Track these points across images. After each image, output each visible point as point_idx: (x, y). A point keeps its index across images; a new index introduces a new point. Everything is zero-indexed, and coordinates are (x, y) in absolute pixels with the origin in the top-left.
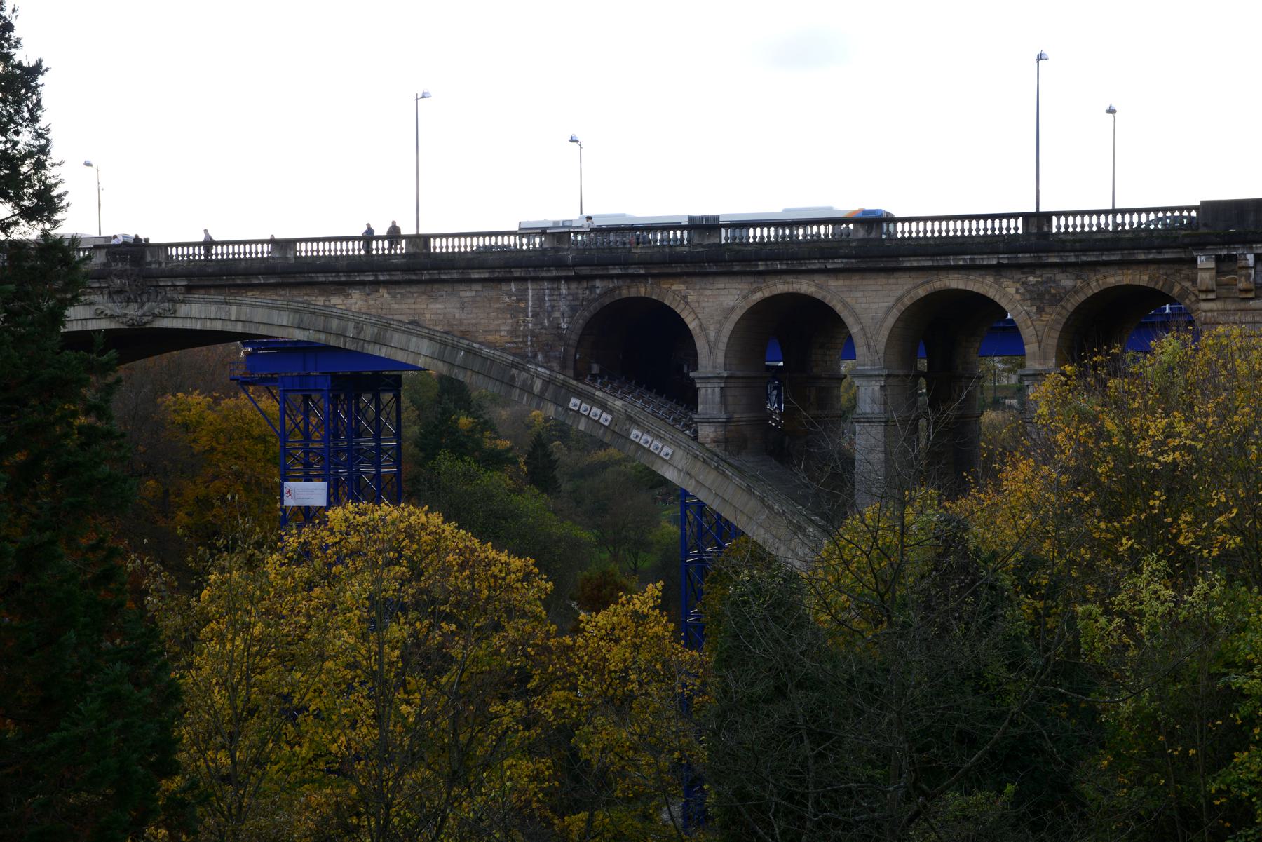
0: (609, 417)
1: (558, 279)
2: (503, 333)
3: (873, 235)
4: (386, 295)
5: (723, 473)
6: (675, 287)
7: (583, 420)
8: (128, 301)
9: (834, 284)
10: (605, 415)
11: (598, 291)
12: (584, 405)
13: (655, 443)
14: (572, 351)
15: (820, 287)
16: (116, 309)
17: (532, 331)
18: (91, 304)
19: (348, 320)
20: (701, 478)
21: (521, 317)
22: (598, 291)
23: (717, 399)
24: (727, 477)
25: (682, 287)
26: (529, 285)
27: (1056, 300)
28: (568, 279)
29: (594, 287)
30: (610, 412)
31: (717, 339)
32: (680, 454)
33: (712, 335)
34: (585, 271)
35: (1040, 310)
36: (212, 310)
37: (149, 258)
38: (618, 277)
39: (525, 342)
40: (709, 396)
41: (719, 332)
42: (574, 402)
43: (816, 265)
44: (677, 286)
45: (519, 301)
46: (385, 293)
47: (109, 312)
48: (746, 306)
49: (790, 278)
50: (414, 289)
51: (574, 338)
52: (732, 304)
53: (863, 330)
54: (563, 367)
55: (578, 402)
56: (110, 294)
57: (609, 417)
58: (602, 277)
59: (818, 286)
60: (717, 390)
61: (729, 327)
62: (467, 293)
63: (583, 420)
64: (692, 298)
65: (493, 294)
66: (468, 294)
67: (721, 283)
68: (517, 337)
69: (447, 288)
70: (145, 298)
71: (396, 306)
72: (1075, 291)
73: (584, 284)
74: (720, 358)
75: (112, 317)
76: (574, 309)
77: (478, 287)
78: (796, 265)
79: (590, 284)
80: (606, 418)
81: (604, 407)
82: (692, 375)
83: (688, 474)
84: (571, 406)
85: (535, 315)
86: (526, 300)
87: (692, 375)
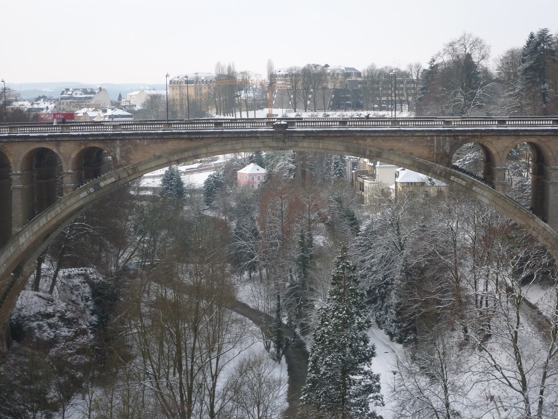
1: (446, 136)
4: (380, 140)
7: (455, 183)
10: (463, 182)
12: (456, 178)
13: (482, 191)
20: (497, 202)
25: (490, 139)
28: (449, 136)
30: (465, 181)
47: (271, 145)
50: (391, 138)
55: (454, 177)
57: (465, 183)
58: (462, 136)
64: (494, 142)
66: (412, 140)
68: (430, 155)
71: (384, 144)
77: (416, 138)
85: (437, 148)
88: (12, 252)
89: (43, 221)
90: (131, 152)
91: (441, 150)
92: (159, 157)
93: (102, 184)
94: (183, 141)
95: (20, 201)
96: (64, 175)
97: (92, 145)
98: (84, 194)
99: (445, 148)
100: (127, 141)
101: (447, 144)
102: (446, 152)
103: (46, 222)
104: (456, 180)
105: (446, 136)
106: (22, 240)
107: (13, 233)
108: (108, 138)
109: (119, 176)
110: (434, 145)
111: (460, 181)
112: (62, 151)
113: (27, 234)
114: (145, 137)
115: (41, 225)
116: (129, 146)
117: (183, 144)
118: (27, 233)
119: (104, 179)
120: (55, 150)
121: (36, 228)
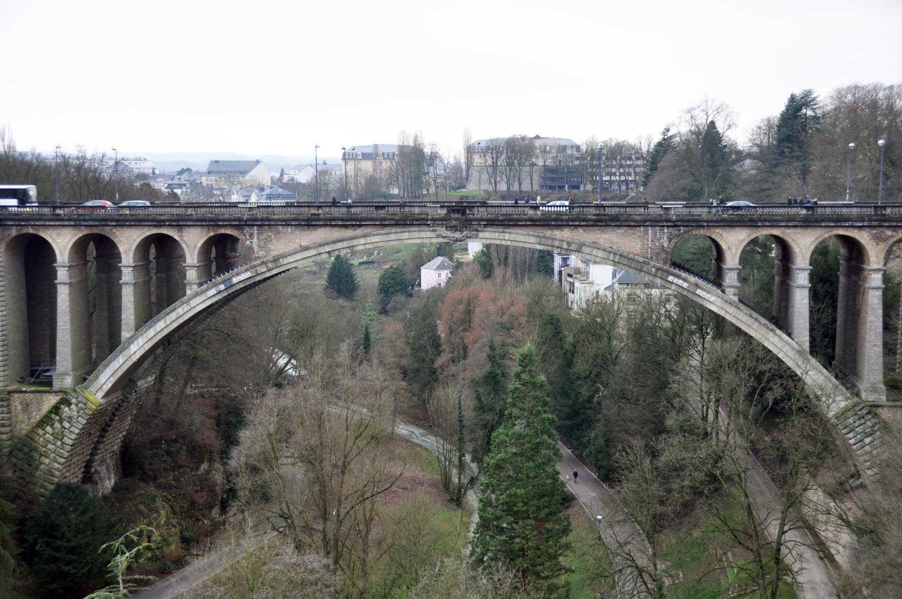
1: (664, 226)
3: (810, 213)
5: (739, 308)
6: (717, 231)
8: (456, 230)
9: (788, 231)
16: (449, 234)
17: (651, 248)
18: (435, 231)
19: (563, 241)
20: (728, 310)
21: (646, 241)
24: (740, 310)
26: (650, 228)
27: (885, 240)
28: (668, 227)
29: (680, 230)
31: (736, 253)
32: (719, 300)
34: (679, 223)
35: (877, 244)
36: (496, 235)
37: (468, 212)
41: (737, 250)
42: (671, 278)
46: (580, 230)
47: (444, 235)
53: (801, 250)
54: (665, 262)
56: (447, 227)
58: (684, 226)
59: (782, 232)
60: (736, 274)
62: (621, 231)
65: (632, 232)
67: (738, 230)
69: (611, 228)
70: (464, 229)
72: (892, 236)
75: (446, 237)
76: (670, 240)
77: (626, 228)
78: (775, 223)
80: (685, 285)
81: (685, 280)
85: (652, 241)
86: (648, 235)
88: (121, 363)
89: (160, 325)
90: (271, 241)
91: (657, 244)
92: (307, 248)
93: (235, 280)
94: (336, 229)
95: (132, 300)
96: (187, 268)
97: (223, 231)
98: (213, 291)
99: (662, 241)
100: (266, 227)
102: (663, 246)
103: (164, 326)
104: (676, 280)
105: (664, 226)
106: (134, 348)
107: (123, 339)
108: (243, 223)
109: (256, 271)
111: (680, 282)
112: (185, 238)
113: (141, 341)
114: (289, 223)
115: (159, 330)
116: (270, 234)
117: (337, 233)
118: (140, 339)
119: (238, 274)
120: (176, 237)
121: (151, 332)
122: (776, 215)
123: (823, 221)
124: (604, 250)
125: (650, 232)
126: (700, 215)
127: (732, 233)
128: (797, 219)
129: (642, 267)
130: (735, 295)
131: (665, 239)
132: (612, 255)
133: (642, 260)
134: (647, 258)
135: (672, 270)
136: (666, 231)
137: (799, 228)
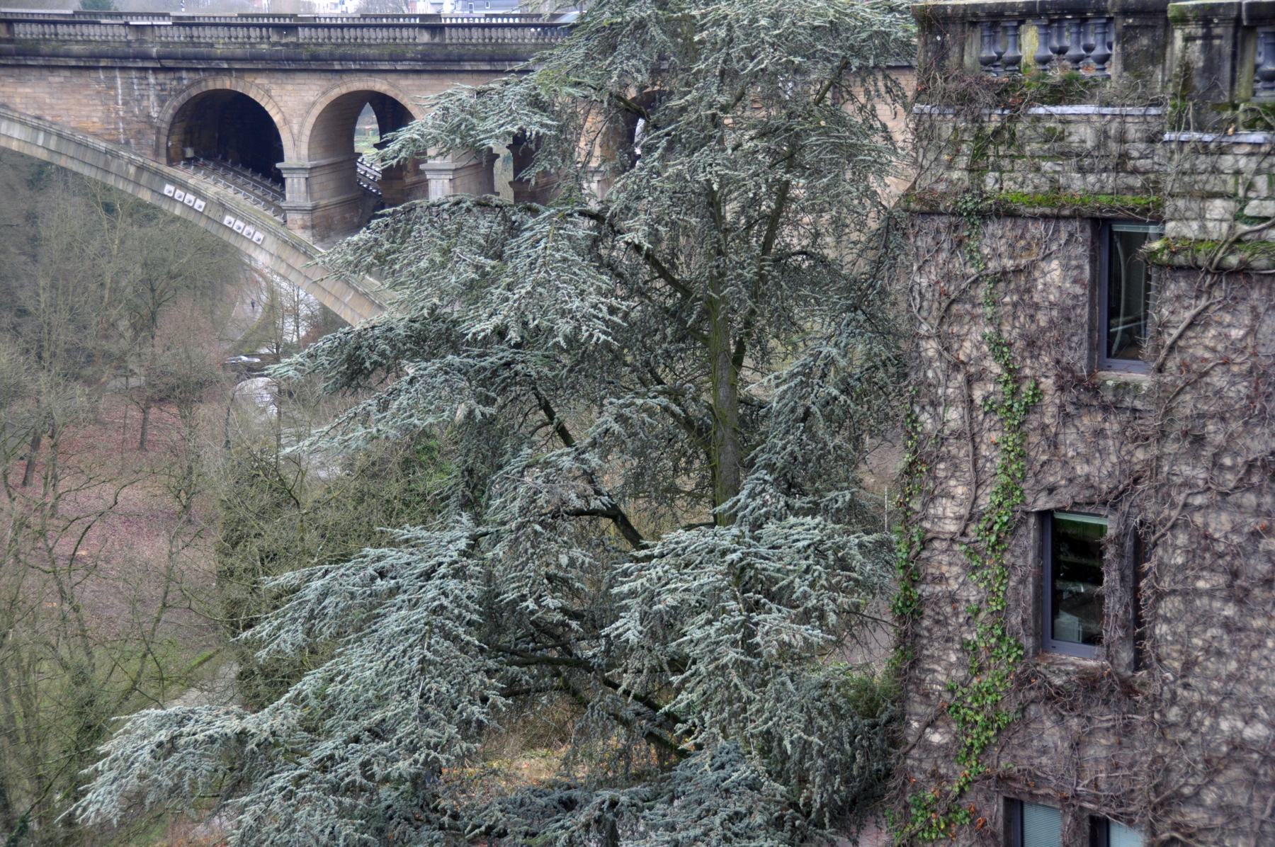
0: (203, 204)
1: (146, 69)
2: (95, 119)
3: (437, 40)
6: (258, 81)
7: (178, 205)
9: (406, 82)
11: (185, 82)
13: (248, 228)
14: (163, 139)
15: (393, 86)
17: (123, 119)
20: (291, 261)
22: (185, 82)
23: (303, 188)
26: (117, 73)
28: (155, 70)
29: (181, 79)
30: (204, 198)
31: (300, 133)
32: (270, 239)
33: (296, 128)
34: (170, 63)
38: (204, 70)
39: (116, 129)
40: (295, 187)
41: (302, 125)
42: (168, 189)
43: (385, 66)
44: (261, 80)
45: (110, 88)
48: (325, 101)
49: (364, 76)
51: (165, 126)
52: (312, 99)
54: (156, 153)
57: (203, 204)
58: (188, 70)
59: (390, 84)
60: (303, 181)
61: (311, 120)
62: (57, 79)
63: (178, 205)
65: (81, 81)
67: (301, 78)
68: (109, 123)
69: (35, 73)
73: (171, 75)
74: (304, 150)
76: (162, 101)
77: (67, 73)
78: (368, 65)
79: (178, 75)
80: (200, 204)
81: (197, 193)
82: (278, 165)
83: (279, 257)
84: (166, 192)
85: (125, 103)
86: (115, 88)
87: (278, 165)
91: (136, 110)
99: (145, 103)
101: (152, 93)
102: (149, 116)
110: (116, 95)
122: (370, 46)
123: (460, 59)
124: (23, 123)
125: (119, 81)
126: (212, 45)
127: (290, 87)
128: (409, 55)
129: (107, 163)
130: (304, 227)
131: (152, 98)
132: (41, 135)
133: (102, 145)
134: (117, 142)
135: (167, 170)
136: (152, 80)
137: (425, 76)
